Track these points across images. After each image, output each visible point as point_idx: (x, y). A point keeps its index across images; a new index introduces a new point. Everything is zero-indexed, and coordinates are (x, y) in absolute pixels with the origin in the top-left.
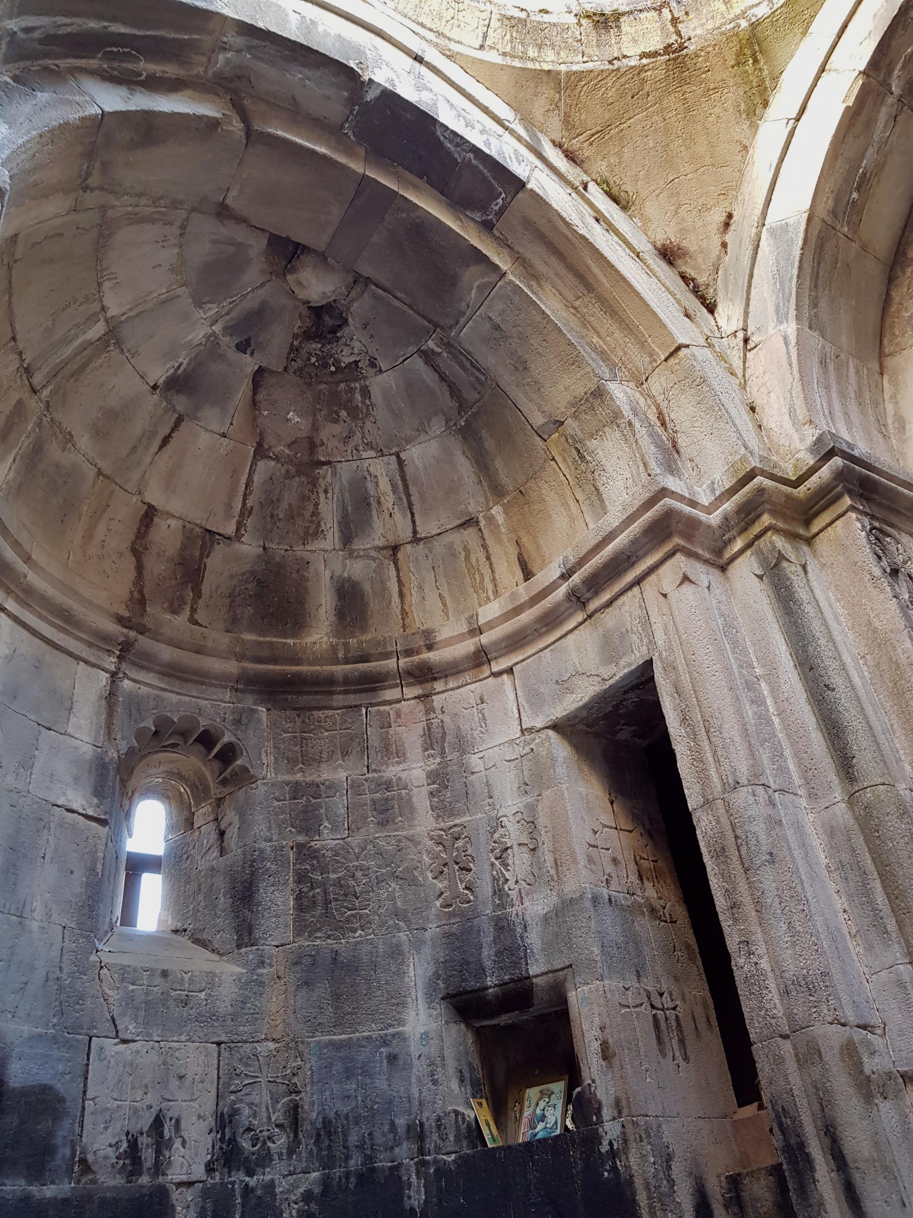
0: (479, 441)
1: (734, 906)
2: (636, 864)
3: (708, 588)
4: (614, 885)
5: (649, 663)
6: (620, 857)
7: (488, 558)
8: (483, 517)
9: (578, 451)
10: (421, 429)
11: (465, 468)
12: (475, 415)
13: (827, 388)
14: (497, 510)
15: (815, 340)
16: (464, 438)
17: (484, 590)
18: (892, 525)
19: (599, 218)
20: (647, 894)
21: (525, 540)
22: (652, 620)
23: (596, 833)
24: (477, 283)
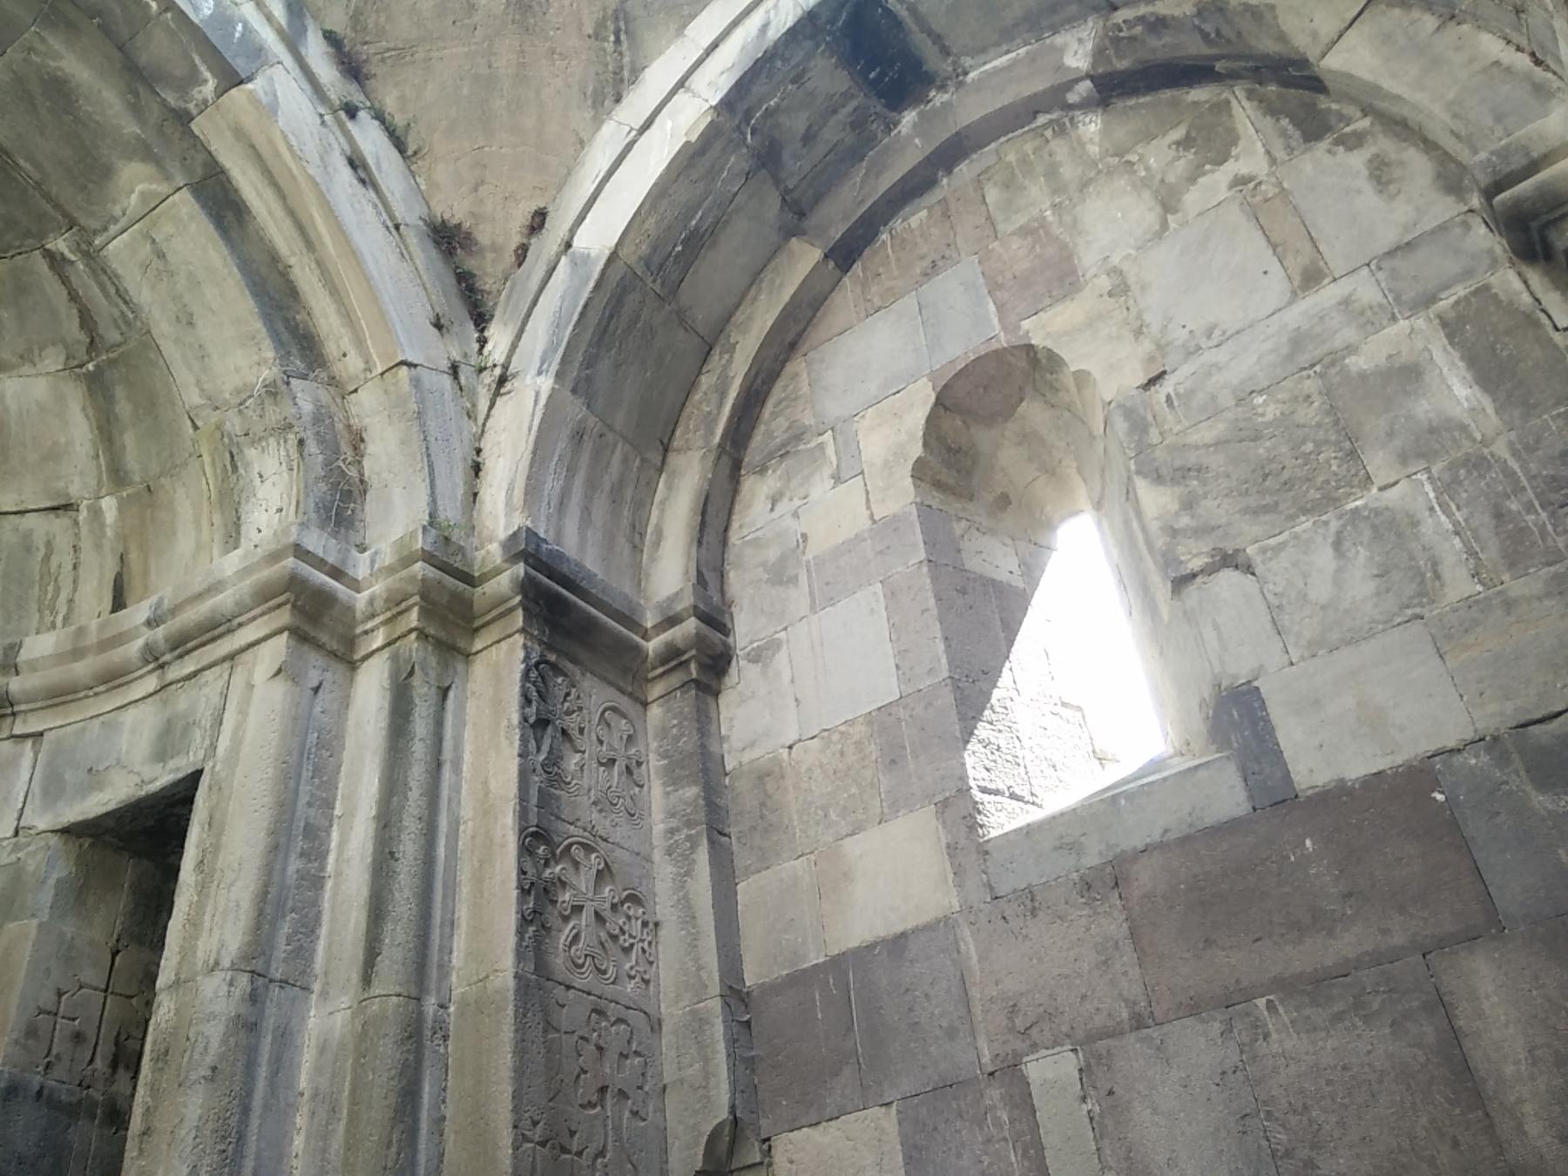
0: (110, 399)
1: (147, 1132)
2: (117, 1043)
3: (316, 690)
4: (58, 1072)
5: (199, 773)
6: (91, 1033)
7: (75, 567)
8: (89, 508)
9: (232, 457)
10: (26, 357)
11: (79, 431)
12: (112, 363)
13: (571, 471)
14: (109, 505)
15: (575, 409)
16: (89, 389)
17: (53, 610)
18: (574, 661)
19: (356, 163)
20: (114, 1088)
21: (133, 556)
22: (226, 716)
23: (60, 994)
24: (139, 188)
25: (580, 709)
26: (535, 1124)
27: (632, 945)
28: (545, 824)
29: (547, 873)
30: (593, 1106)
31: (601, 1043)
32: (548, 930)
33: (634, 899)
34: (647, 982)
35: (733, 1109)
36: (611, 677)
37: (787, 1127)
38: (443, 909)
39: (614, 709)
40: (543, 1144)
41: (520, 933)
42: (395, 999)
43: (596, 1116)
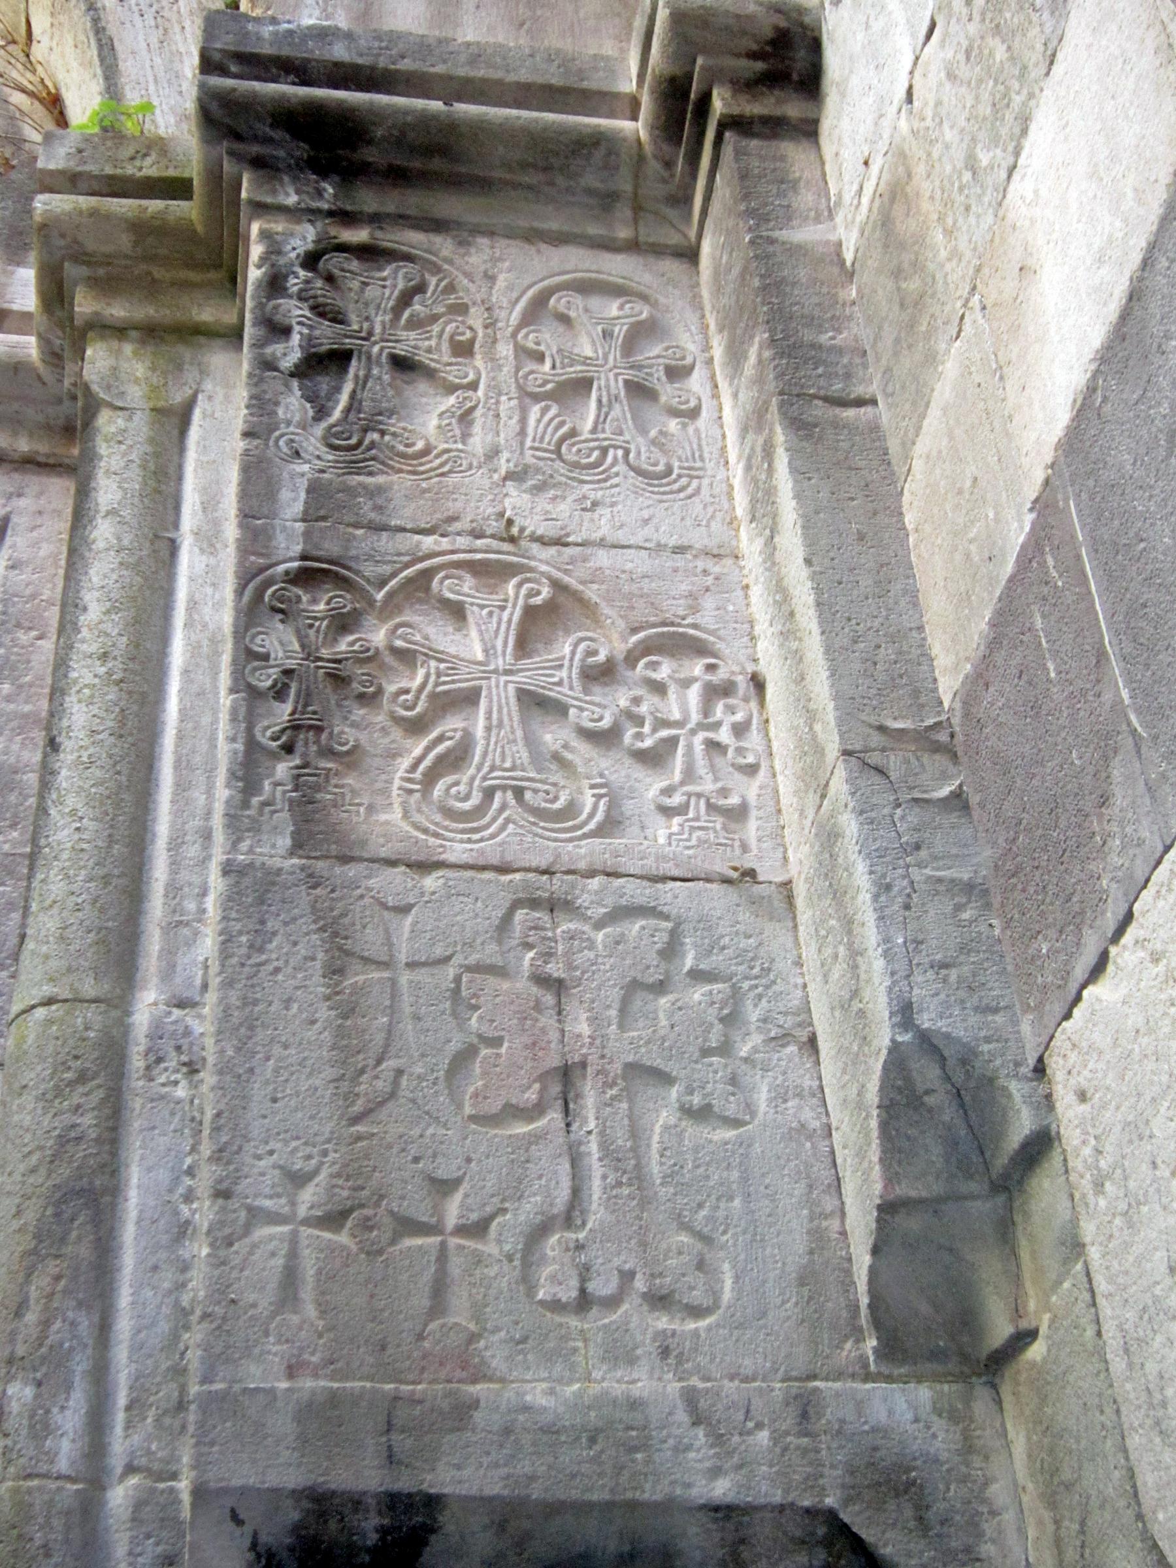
18: (437, 225)
25: (461, 309)
26: (299, 1179)
27: (673, 742)
28: (331, 547)
29: (343, 646)
30: (537, 1110)
31: (555, 969)
32: (351, 758)
33: (683, 645)
34: (739, 814)
35: (905, 1013)
36: (554, 225)
37: (1058, 1009)
38: (177, 813)
39: (586, 287)
40: (334, 1219)
41: (247, 775)
42: (40, 1013)
43: (536, 1138)
